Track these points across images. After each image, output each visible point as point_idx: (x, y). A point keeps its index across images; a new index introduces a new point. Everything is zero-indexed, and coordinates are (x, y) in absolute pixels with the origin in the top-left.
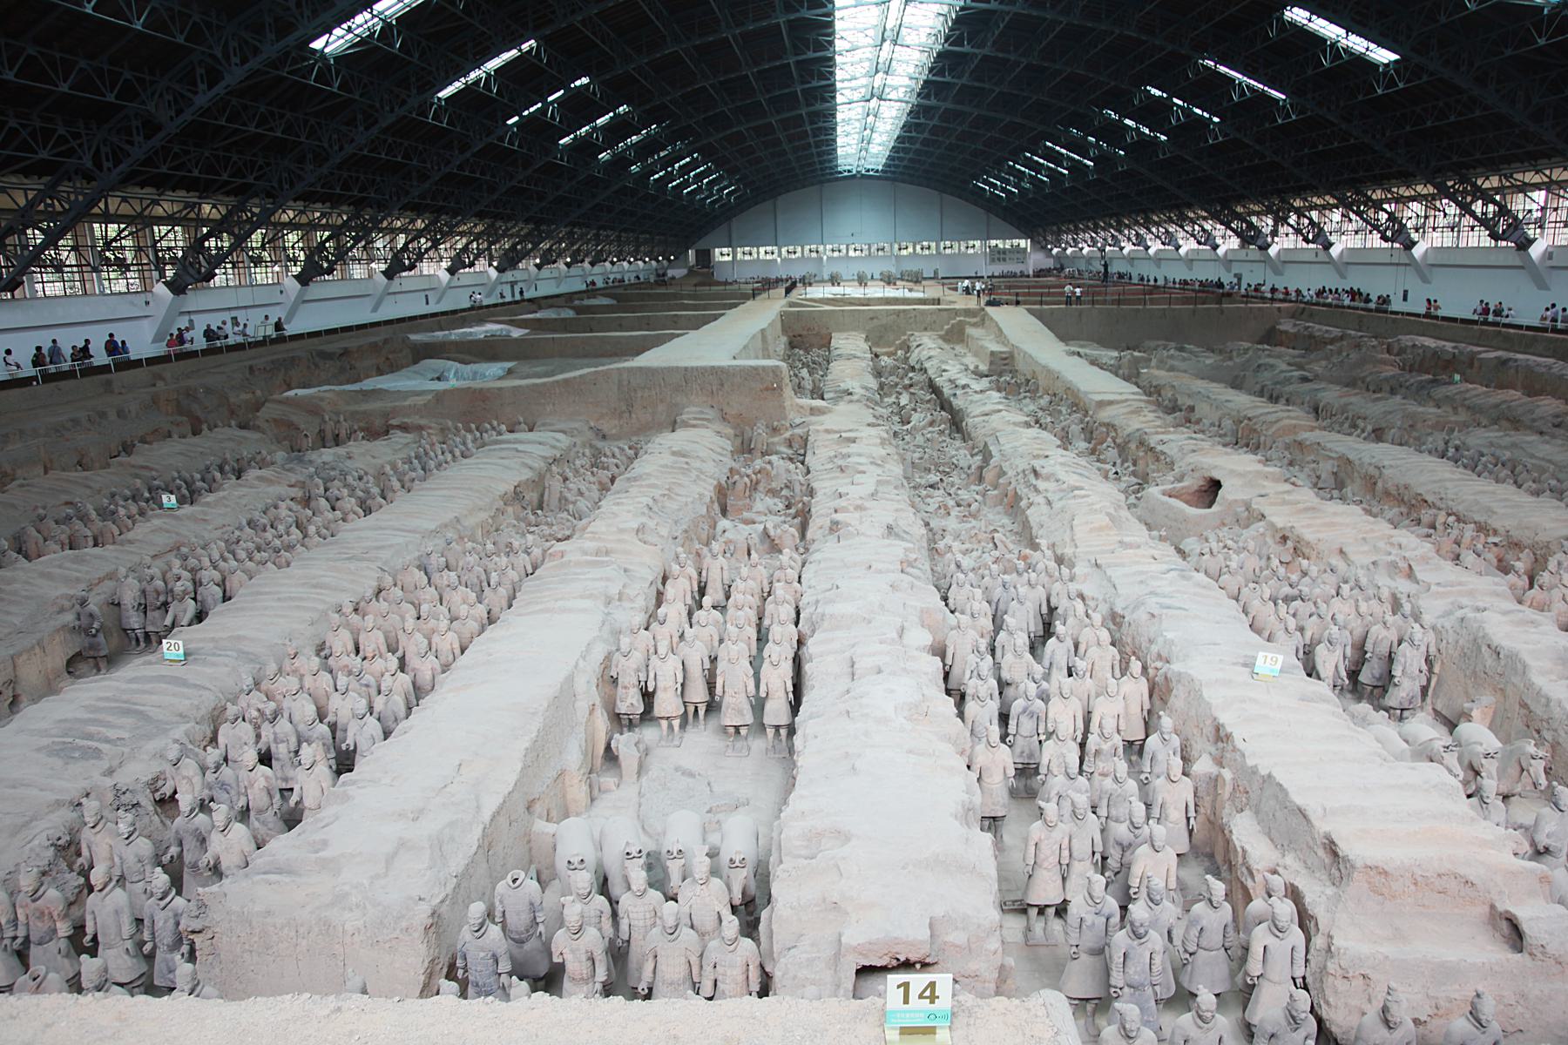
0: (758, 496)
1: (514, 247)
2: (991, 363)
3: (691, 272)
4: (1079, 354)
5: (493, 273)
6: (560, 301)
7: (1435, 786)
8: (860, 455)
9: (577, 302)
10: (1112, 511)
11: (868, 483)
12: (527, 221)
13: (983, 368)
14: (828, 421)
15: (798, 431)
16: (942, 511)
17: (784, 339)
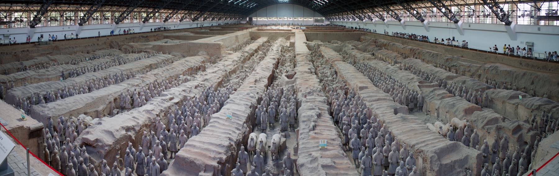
0: (200, 71)
1: (196, 16)
2: (290, 45)
3: (247, 22)
4: (306, 43)
5: (191, 21)
6: (207, 28)
7: (219, 145)
8: (221, 64)
9: (212, 28)
10: (258, 79)
11: (216, 69)
12: (198, 11)
13: (288, 45)
14: (230, 56)
15: (222, 58)
16: (237, 77)
17: (249, 38)
